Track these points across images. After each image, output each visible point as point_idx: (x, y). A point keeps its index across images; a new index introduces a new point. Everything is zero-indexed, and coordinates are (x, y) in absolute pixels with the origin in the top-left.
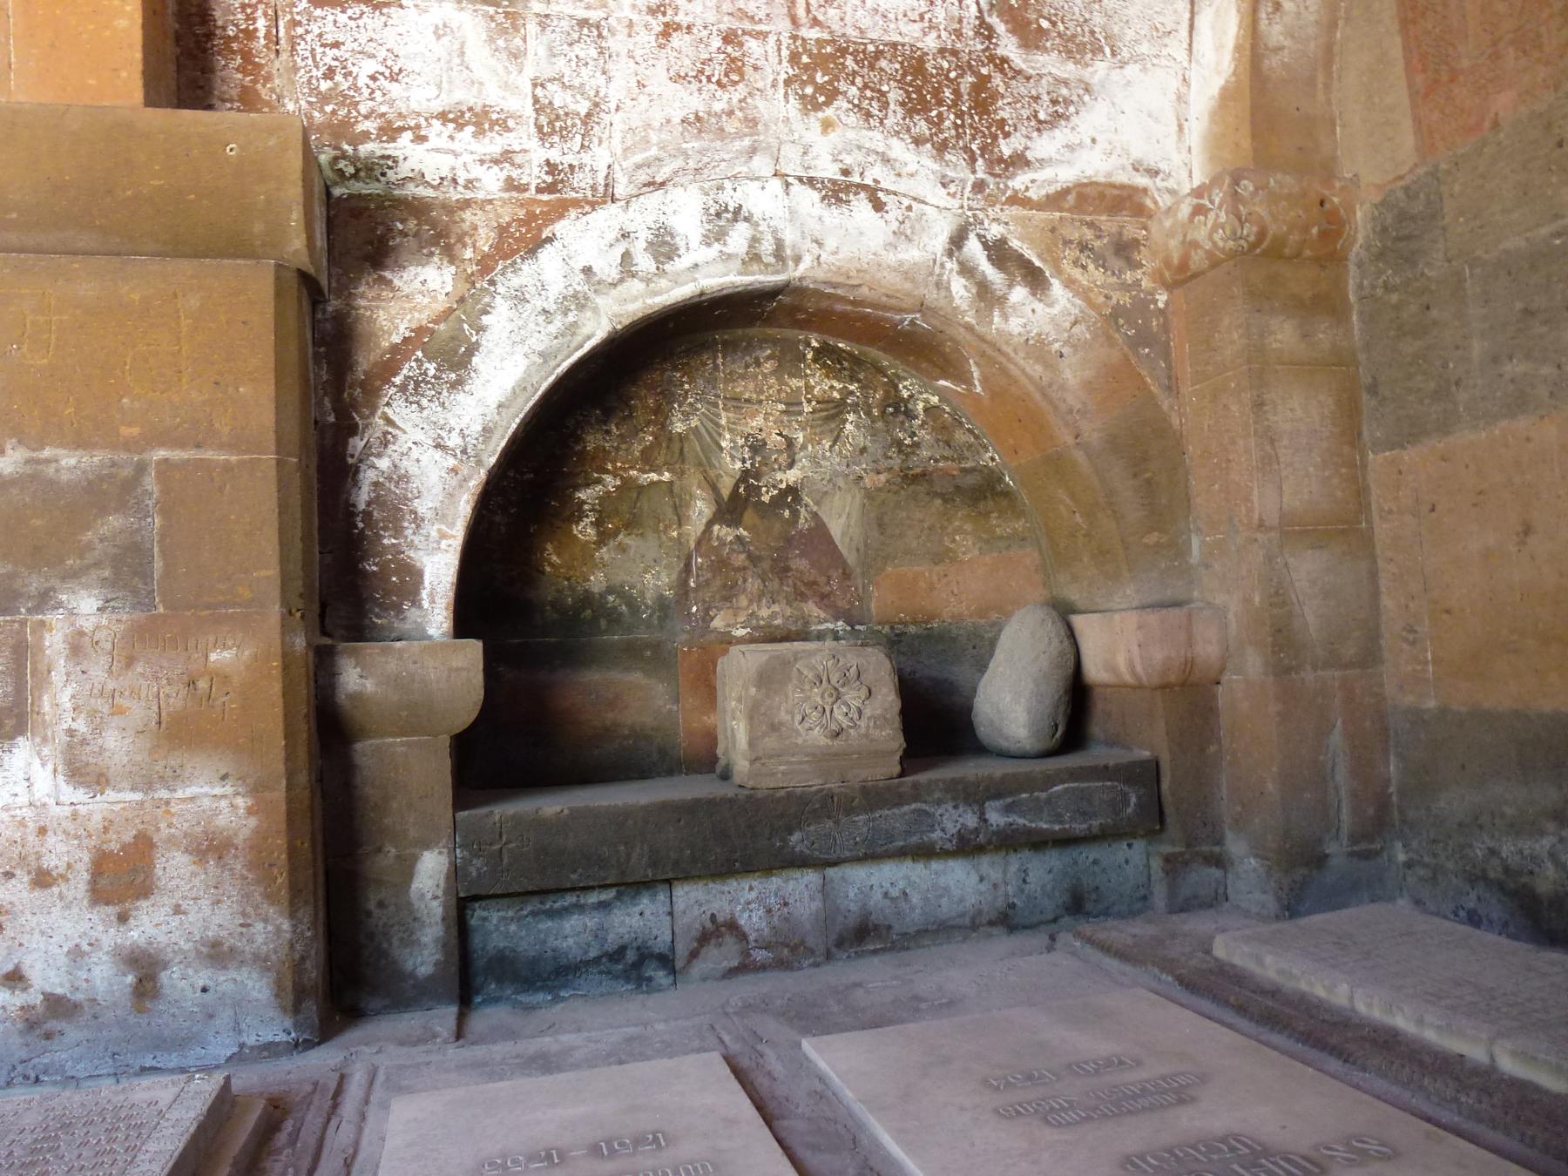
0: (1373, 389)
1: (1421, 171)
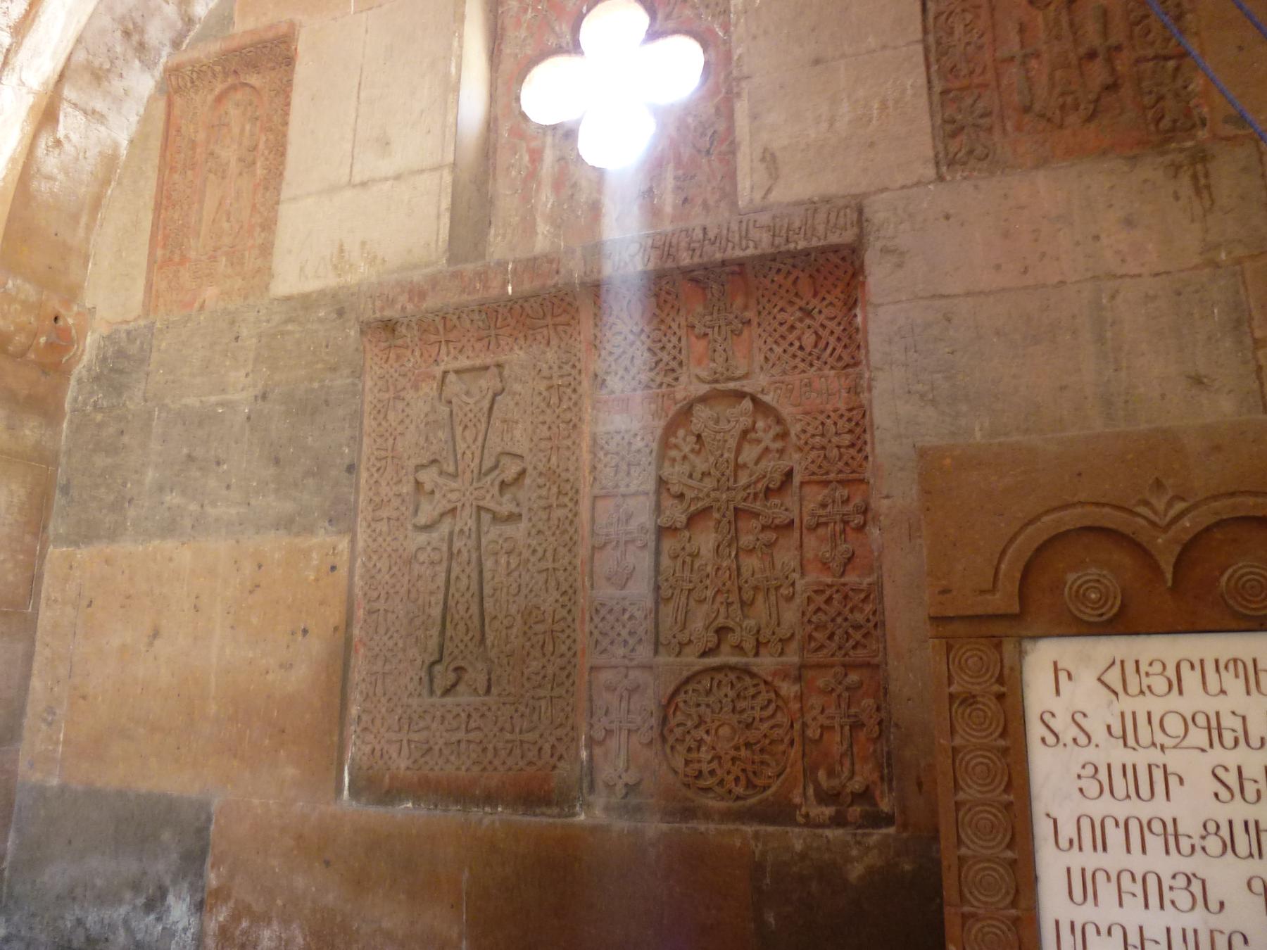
0: (66, 490)
1: (142, 323)
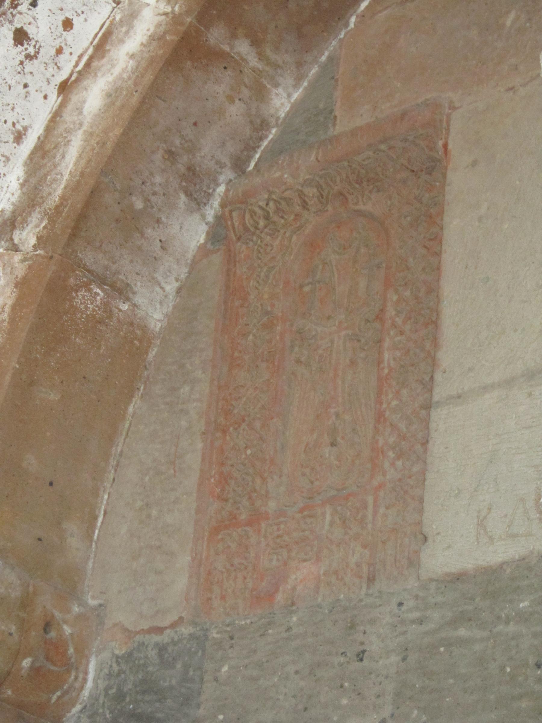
1: (186, 630)
